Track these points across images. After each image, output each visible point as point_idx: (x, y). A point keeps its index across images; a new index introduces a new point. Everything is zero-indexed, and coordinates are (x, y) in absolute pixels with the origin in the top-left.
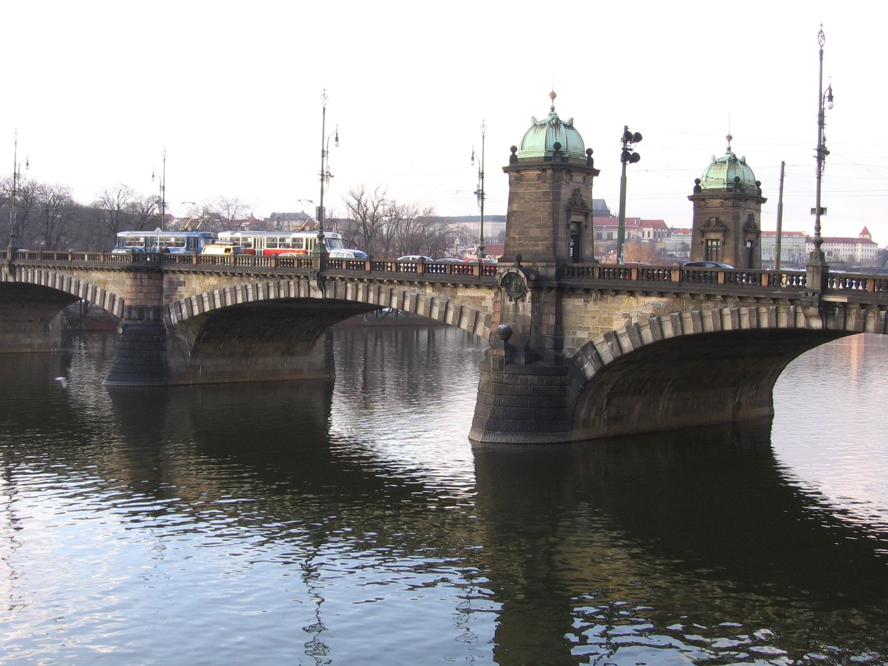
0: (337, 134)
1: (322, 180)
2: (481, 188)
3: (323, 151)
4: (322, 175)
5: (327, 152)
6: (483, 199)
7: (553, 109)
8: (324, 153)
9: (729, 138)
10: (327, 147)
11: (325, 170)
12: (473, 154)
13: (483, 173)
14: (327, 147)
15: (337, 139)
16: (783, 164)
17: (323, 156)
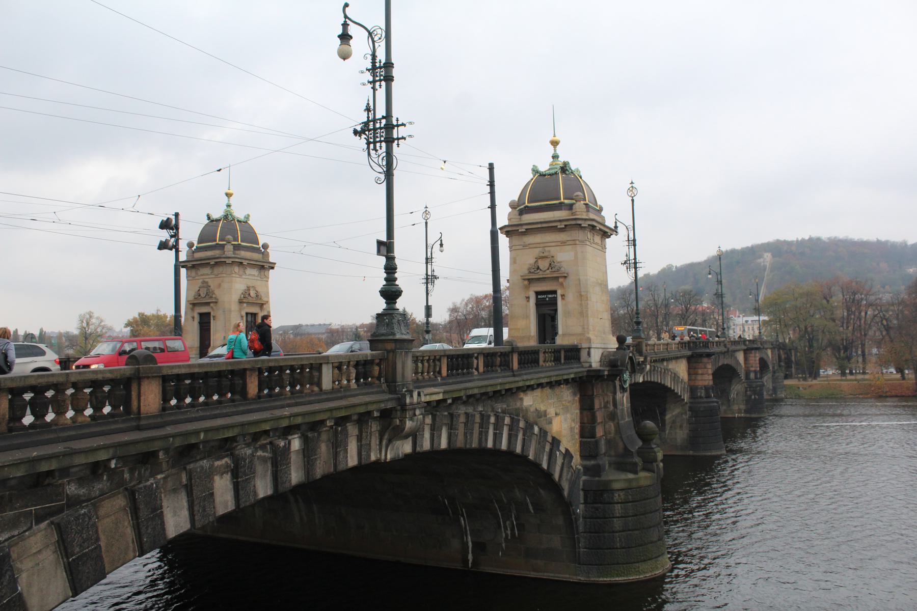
0: (441, 241)
1: (427, 283)
2: (632, 257)
3: (427, 259)
4: (427, 279)
5: (432, 258)
6: (636, 268)
7: (229, 206)
8: (428, 260)
9: (555, 143)
10: (431, 254)
11: (429, 273)
12: (616, 223)
13: (634, 240)
14: (431, 254)
15: (441, 245)
16: (491, 167)
17: (427, 263)
